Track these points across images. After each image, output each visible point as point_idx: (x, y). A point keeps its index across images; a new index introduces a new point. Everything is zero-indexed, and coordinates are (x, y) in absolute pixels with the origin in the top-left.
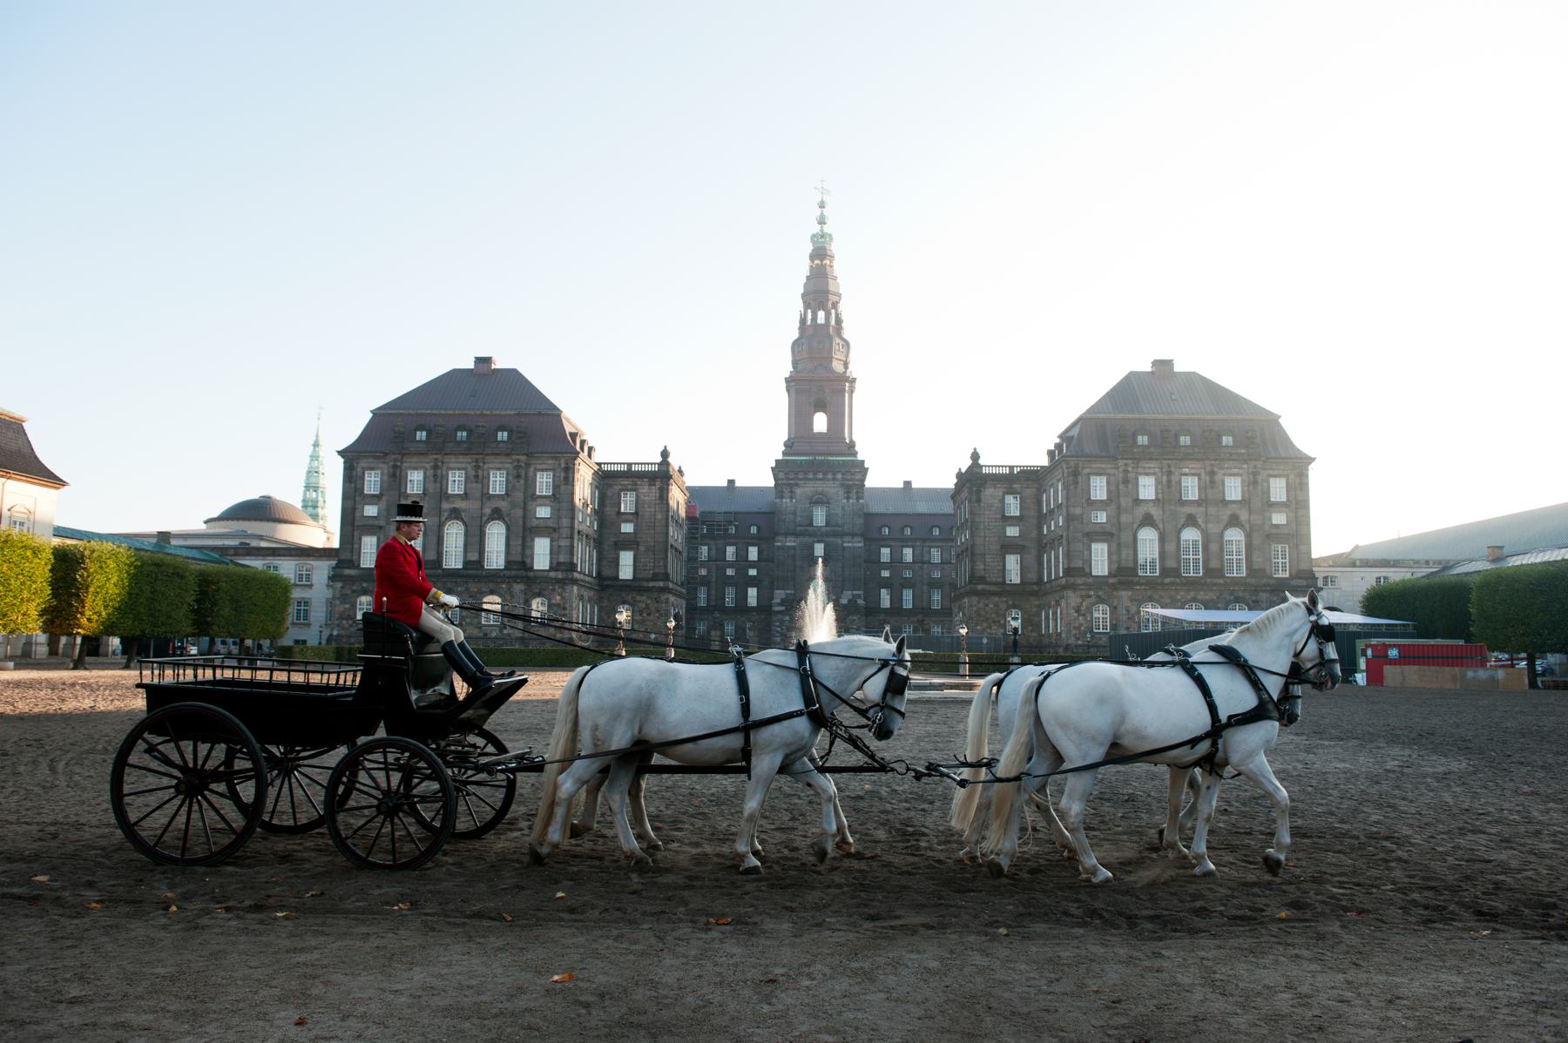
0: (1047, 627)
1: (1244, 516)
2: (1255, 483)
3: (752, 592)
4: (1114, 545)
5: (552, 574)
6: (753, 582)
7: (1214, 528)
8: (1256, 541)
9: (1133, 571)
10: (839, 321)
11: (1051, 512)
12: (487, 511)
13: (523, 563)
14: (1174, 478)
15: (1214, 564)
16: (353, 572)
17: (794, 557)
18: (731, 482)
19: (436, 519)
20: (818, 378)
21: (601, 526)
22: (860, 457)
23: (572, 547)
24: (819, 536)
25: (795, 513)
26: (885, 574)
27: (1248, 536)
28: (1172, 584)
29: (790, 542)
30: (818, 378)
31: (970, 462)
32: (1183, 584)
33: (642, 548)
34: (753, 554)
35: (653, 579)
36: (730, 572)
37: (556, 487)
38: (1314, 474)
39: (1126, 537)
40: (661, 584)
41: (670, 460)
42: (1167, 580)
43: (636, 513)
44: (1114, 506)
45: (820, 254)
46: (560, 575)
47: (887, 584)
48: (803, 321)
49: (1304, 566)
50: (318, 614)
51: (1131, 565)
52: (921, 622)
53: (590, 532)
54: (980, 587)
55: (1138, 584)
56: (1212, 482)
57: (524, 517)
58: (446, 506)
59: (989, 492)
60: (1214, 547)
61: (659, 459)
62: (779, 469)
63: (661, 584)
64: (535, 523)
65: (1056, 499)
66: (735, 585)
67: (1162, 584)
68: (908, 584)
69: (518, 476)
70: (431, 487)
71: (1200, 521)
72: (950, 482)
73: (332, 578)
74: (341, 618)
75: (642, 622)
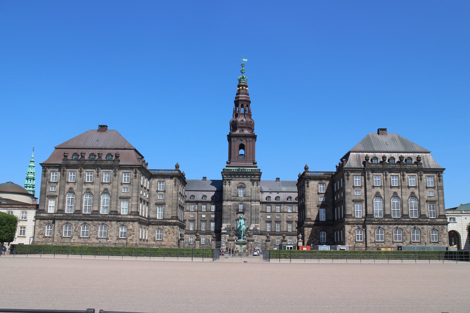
0: (337, 239)
1: (417, 193)
2: (421, 179)
3: (213, 224)
5: (129, 217)
7: (405, 198)
8: (422, 203)
9: (372, 216)
10: (249, 111)
11: (338, 191)
12: (102, 189)
13: (117, 212)
14: (388, 177)
15: (405, 212)
16: (44, 215)
17: (230, 209)
18: (205, 178)
19: (80, 193)
20: (241, 136)
21: (149, 196)
24: (241, 202)
25: (231, 191)
26: (269, 217)
27: (419, 201)
29: (229, 203)
30: (241, 136)
32: (392, 221)
33: (167, 206)
35: (171, 219)
36: (204, 216)
37: (132, 179)
38: (445, 175)
39: (369, 202)
40: (175, 221)
41: (180, 169)
42: (386, 219)
43: (165, 191)
44: (363, 188)
45: (241, 85)
46: (132, 217)
47: (269, 222)
48: (235, 111)
49: (442, 213)
50: (29, 232)
51: (371, 213)
52: (284, 237)
54: (309, 223)
55: (374, 221)
56: (404, 179)
57: (117, 192)
58: (85, 187)
59: (313, 184)
60: (405, 206)
61: (175, 168)
62: (224, 173)
63: (175, 221)
64: (122, 195)
66: (206, 221)
68: (278, 222)
69: (115, 175)
70: (79, 179)
71: (399, 195)
72: (296, 179)
73: (36, 218)
74: (39, 234)
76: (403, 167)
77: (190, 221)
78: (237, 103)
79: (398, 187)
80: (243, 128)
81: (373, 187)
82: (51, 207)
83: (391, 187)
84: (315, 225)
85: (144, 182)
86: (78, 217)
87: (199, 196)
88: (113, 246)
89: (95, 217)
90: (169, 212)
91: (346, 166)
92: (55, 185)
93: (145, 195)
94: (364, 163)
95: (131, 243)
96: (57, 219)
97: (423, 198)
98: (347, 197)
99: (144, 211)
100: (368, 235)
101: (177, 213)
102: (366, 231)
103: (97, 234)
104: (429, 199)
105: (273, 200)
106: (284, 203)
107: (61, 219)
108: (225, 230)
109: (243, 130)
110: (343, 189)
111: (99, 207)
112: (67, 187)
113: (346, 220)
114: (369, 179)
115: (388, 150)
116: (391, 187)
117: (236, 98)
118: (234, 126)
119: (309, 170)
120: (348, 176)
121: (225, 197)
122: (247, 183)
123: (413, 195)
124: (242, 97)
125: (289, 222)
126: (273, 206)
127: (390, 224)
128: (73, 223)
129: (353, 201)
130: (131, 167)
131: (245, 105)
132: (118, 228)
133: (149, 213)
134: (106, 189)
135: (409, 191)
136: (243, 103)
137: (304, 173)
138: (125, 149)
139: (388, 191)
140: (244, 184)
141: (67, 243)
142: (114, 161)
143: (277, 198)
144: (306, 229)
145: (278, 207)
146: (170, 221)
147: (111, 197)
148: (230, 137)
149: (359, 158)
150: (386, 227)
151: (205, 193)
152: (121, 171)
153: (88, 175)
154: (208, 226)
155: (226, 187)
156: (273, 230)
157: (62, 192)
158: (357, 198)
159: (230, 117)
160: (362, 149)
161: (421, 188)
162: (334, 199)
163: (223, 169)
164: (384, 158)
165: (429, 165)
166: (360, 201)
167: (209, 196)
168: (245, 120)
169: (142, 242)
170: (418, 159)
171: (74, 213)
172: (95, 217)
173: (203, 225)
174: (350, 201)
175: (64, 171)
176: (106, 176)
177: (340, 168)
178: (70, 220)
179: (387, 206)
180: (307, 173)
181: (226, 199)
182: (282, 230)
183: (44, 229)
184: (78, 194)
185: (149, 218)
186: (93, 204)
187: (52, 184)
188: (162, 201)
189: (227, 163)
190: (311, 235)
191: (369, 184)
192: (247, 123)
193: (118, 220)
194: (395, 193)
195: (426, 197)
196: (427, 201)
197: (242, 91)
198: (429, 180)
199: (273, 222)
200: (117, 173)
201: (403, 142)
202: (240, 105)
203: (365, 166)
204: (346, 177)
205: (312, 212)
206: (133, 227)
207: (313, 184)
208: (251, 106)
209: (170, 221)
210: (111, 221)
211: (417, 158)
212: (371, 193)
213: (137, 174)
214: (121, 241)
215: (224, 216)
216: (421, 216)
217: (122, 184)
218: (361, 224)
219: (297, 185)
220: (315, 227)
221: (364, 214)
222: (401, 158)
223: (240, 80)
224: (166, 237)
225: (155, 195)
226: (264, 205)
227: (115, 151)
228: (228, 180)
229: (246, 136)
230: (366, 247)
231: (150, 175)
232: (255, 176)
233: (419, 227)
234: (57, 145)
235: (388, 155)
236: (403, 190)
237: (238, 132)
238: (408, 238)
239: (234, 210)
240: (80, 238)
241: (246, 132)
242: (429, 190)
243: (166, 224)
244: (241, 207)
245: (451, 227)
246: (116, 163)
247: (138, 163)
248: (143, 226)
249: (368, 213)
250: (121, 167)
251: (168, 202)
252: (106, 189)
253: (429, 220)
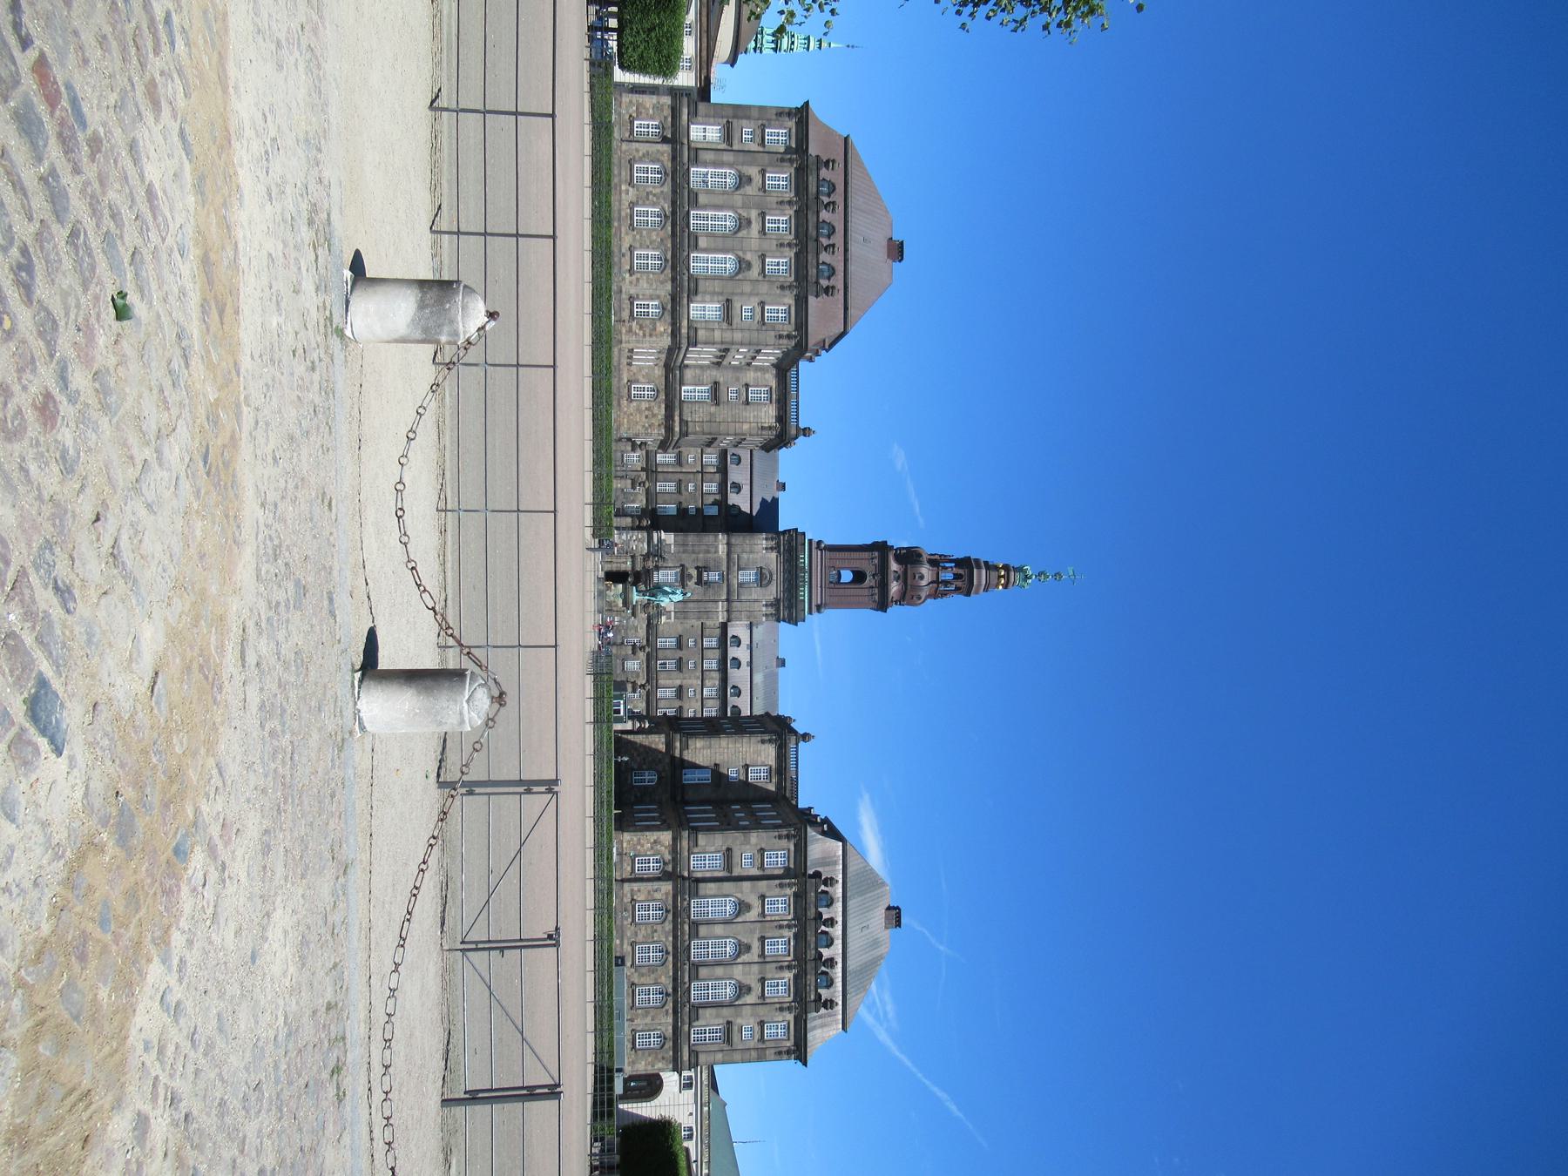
0: (641, 811)
1: (750, 999)
2: (781, 1009)
4: (721, 874)
5: (685, 323)
7: (738, 971)
8: (727, 1013)
10: (944, 594)
12: (748, 257)
16: (685, 117)
18: (782, 487)
19: (740, 204)
20: (882, 574)
21: (735, 367)
24: (726, 578)
28: (683, 933)
29: (722, 549)
30: (882, 574)
32: (683, 941)
33: (713, 409)
36: (691, 487)
38: (792, 1065)
39: (728, 886)
41: (801, 438)
43: (747, 403)
44: (755, 872)
46: (684, 331)
47: (680, 645)
49: (702, 1058)
51: (701, 892)
56: (781, 968)
58: (754, 214)
59: (767, 754)
60: (719, 971)
61: (802, 426)
62: (795, 536)
64: (737, 305)
65: (765, 818)
66: (679, 492)
67: (683, 923)
69: (782, 288)
70: (773, 200)
71: (744, 958)
72: (783, 711)
75: (638, 410)
76: (810, 966)
77: (679, 457)
78: (966, 564)
79: (762, 955)
80: (903, 578)
81: (763, 897)
82: (704, 133)
83: (762, 939)
84: (673, 757)
85: (769, 356)
86: (681, 198)
87: (737, 474)
88: (614, 288)
89: (680, 239)
90: (697, 416)
91: (811, 832)
92: (758, 140)
93: (737, 357)
94: (817, 875)
96: (674, 150)
97: (738, 1015)
98: (738, 835)
99: (699, 356)
100: (649, 886)
102: (658, 879)
103: (641, 247)
104: (735, 1028)
105: (733, 652)
106: (724, 680)
107: (674, 158)
108: (660, 539)
109: (897, 579)
110: (757, 825)
111: (705, 250)
112: (753, 171)
113: (685, 834)
114: (781, 886)
115: (849, 931)
116: (762, 939)
117: (977, 561)
118: (910, 557)
119: (801, 744)
120: (788, 837)
121: (737, 539)
122: (772, 592)
123: (743, 989)
124: (980, 576)
125: (680, 691)
126: (717, 654)
127: (675, 937)
128: (667, 188)
129: (729, 850)
130: (802, 324)
131: (959, 583)
132: (658, 297)
133: (695, 366)
134: (749, 265)
135: (753, 981)
136: (966, 578)
137: (795, 732)
138: (846, 309)
139: (752, 932)
141: (619, 174)
142: (817, 283)
143: (737, 663)
144: (662, 738)
145: (714, 666)
146: (677, 418)
147: (731, 278)
148: (881, 548)
149: (828, 861)
150: (668, 926)
151: (746, 489)
152: (792, 302)
153: (780, 221)
154: (667, 497)
155: (761, 541)
156: (660, 654)
157: (741, 157)
158: (736, 859)
159: (929, 548)
160: (851, 870)
161: (762, 1010)
162: (733, 804)
164: (831, 922)
165: (814, 1028)
166: (729, 865)
167: (740, 501)
168: (924, 583)
169: (626, 353)
170: (829, 1004)
171: (690, 191)
172: (680, 239)
173: (670, 487)
174: (729, 843)
175: (791, 161)
176: (780, 264)
177: (808, 818)
178: (673, 179)
179: (719, 930)
181: (733, 541)
182: (661, 675)
183: (652, 118)
184: (738, 199)
185: (683, 367)
186: (714, 236)
187: (758, 132)
188: (723, 398)
189: (819, 542)
190: (648, 750)
192: (918, 588)
193: (675, 298)
194: (748, 948)
195: (739, 1021)
196: (729, 1023)
197: (994, 574)
198: (779, 1028)
199: (679, 654)
200: (787, 292)
201: (870, 967)
202: (961, 571)
203: (811, 876)
204: (784, 832)
205: (702, 752)
206: (662, 334)
207: (768, 754)
208: (958, 598)
209: (677, 418)
210: (673, 280)
211: (832, 1001)
212: (747, 891)
213: (785, 341)
214: (626, 304)
215: (692, 538)
216: (696, 1010)
217: (762, 304)
218: (674, 868)
219: (767, 714)
220: (667, 760)
221: (699, 875)
222: (831, 962)
223: (1020, 570)
224: (638, 410)
225: (738, 379)
226: (718, 632)
227: (840, 286)
228: (778, 544)
229: (883, 586)
230: (623, 881)
231: (784, 369)
232: (788, 609)
233: (670, 1006)
234: (853, 138)
235: (837, 931)
236: (755, 968)
237: (894, 566)
238: (643, 980)
239: (706, 560)
240: (632, 205)
241: (894, 588)
242: (757, 1028)
243: (669, 409)
244: (713, 576)
245: (670, 1080)
246: (812, 288)
247: (812, 341)
248: (663, 356)
249: (702, 885)
250: (801, 304)
251: (722, 413)
252: (749, 265)
253: (686, 1028)
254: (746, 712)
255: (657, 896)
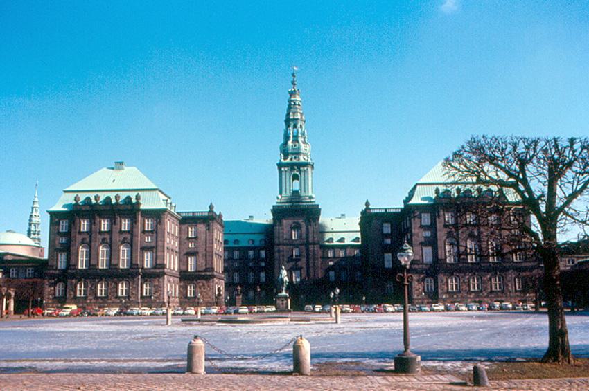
3: (263, 275)
6: (262, 269)
12: (121, 239)
17: (283, 256)
22: (316, 203)
23: (164, 255)
31: (365, 207)
33: (200, 255)
34: (263, 253)
35: (205, 271)
41: (214, 210)
43: (196, 238)
51: (443, 257)
53: (174, 248)
64: (145, 245)
95: (158, 301)
101: (212, 263)
103: (117, 292)
119: (370, 207)
121: (277, 241)
140: (297, 223)
148: (280, 166)
163: (273, 206)
180: (368, 211)
191: (440, 222)
209: (203, 274)
254: (359, 235)
255: (445, 280)
